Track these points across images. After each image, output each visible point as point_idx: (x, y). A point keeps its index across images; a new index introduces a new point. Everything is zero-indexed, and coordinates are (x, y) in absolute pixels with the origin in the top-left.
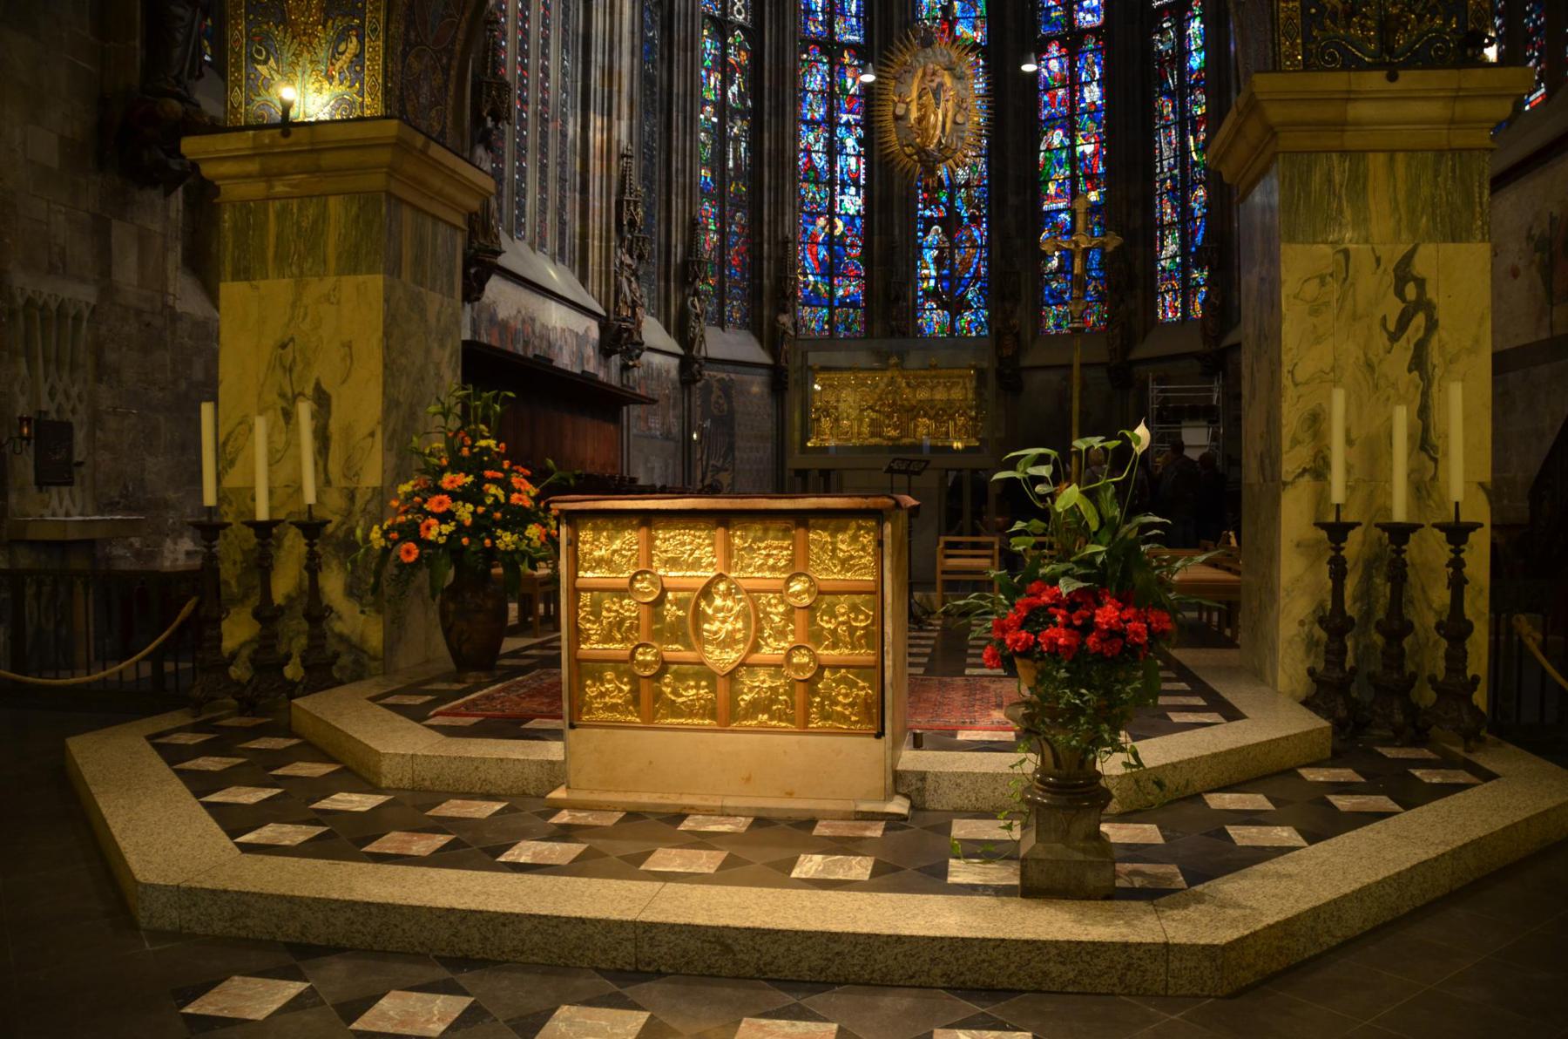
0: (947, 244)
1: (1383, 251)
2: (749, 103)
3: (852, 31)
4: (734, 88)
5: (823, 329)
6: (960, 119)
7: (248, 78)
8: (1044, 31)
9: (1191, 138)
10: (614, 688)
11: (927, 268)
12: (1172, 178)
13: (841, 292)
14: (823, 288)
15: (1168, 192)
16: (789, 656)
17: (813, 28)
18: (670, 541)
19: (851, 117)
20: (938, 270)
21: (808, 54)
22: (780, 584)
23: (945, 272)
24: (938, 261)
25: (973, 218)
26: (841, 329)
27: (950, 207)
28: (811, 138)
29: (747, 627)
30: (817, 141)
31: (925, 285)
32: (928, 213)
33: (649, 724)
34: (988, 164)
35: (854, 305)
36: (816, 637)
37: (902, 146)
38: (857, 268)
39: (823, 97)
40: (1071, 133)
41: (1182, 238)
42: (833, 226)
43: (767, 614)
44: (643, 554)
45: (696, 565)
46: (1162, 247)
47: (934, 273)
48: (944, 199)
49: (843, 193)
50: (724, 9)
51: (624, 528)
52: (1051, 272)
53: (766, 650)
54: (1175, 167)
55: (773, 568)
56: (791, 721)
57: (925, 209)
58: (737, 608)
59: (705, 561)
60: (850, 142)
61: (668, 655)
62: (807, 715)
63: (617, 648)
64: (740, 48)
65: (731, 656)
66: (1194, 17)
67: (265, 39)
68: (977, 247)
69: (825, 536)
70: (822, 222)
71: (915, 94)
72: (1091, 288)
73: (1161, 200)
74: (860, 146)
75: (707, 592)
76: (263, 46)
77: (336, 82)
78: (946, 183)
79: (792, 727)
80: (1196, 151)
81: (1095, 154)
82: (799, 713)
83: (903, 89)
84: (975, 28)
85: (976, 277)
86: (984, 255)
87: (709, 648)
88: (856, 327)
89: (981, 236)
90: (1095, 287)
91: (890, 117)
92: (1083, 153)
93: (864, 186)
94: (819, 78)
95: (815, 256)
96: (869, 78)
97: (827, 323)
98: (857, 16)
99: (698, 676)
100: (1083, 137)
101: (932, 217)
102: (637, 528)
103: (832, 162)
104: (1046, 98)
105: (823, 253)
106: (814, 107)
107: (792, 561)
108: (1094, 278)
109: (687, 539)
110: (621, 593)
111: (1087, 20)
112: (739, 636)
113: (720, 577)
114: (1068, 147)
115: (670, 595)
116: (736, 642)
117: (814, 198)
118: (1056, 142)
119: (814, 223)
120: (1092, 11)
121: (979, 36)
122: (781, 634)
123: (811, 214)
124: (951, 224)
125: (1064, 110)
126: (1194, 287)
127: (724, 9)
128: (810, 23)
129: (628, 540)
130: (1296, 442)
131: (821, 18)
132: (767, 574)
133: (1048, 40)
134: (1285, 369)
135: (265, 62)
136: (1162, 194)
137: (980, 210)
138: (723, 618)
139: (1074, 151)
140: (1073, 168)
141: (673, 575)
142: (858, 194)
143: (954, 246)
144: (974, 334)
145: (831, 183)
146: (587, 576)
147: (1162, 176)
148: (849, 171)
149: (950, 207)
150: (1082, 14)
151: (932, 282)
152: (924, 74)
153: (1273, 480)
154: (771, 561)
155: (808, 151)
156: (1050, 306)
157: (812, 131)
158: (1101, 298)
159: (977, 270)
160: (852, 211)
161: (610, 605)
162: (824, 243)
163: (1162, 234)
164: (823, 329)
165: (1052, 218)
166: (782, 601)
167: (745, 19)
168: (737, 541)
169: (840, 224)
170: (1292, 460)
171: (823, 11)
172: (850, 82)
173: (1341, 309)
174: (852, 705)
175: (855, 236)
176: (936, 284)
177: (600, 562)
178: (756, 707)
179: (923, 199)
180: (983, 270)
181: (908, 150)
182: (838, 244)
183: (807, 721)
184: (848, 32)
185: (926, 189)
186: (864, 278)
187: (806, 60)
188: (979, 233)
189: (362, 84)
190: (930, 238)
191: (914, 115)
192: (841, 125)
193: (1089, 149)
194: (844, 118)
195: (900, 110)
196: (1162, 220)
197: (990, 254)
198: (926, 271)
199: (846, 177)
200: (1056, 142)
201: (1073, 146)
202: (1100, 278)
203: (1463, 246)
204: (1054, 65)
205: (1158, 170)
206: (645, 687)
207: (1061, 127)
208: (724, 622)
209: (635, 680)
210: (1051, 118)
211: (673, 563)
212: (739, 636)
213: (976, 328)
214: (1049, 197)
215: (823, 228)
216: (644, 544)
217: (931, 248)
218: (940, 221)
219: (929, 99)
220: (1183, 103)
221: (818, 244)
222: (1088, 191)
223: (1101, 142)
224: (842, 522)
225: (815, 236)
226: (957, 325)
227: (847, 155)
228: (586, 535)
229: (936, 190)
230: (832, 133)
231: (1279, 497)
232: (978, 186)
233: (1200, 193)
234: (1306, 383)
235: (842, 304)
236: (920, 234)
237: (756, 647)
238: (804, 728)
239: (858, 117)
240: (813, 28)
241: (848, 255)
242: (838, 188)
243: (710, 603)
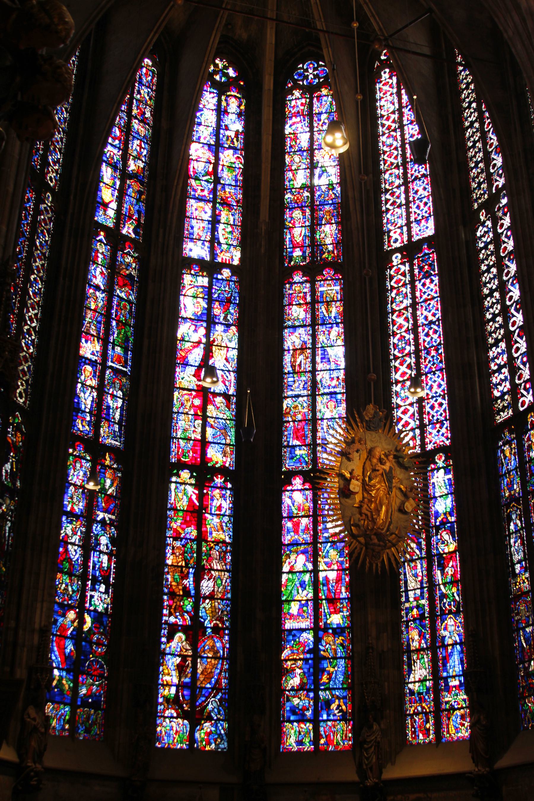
0: (190, 653)
2: (18, 484)
3: (114, 438)
4: (8, 466)
5: (63, 729)
8: (289, 465)
9: (439, 572)
11: (168, 674)
12: (418, 607)
13: (84, 691)
14: (67, 684)
15: (414, 620)
17: (80, 426)
19: (107, 516)
20: (180, 677)
21: (74, 450)
23: (187, 680)
24: (181, 668)
25: (215, 629)
26: (81, 731)
27: (195, 616)
28: (69, 532)
30: (74, 533)
31: (166, 692)
32: (172, 619)
34: (234, 580)
35: (96, 705)
38: (102, 666)
39: (83, 493)
40: (314, 557)
41: (434, 661)
42: (82, 622)
46: (410, 670)
47: (176, 681)
48: (189, 608)
49: (94, 589)
52: (292, 689)
54: (422, 596)
57: (170, 614)
60: (104, 540)
64: (17, 429)
66: (438, 469)
68: (219, 658)
70: (71, 615)
72: (334, 706)
73: (407, 627)
74: (113, 546)
78: (193, 592)
80: (445, 584)
81: (339, 580)
84: (225, 454)
85: (217, 688)
86: (226, 667)
88: (96, 729)
89: (224, 648)
90: (339, 706)
92: (326, 578)
93: (113, 585)
94: (81, 473)
95: (62, 649)
97: (68, 722)
100: (326, 563)
101: (176, 624)
103: (86, 557)
104: (289, 525)
105: (70, 647)
106: (75, 500)
108: (338, 698)
114: (311, 572)
117: (66, 589)
118: (299, 567)
119: (64, 615)
121: (229, 461)
123: (61, 605)
125: (307, 537)
126: (448, 710)
128: (79, 421)
131: (88, 419)
133: (292, 474)
136: (408, 621)
137: (223, 623)
139: (316, 577)
140: (316, 591)
142: (106, 592)
143: (196, 656)
144: (213, 746)
145: (84, 577)
147: (407, 605)
148: (101, 567)
149: (195, 616)
150: (325, 456)
151: (173, 690)
155: (65, 543)
156: (292, 722)
157: (71, 523)
158: (344, 718)
159: (218, 681)
160: (100, 609)
162: (72, 637)
163: (409, 658)
164: (63, 729)
165: (294, 636)
167: (24, 403)
169: (88, 619)
171: (90, 413)
172: (108, 482)
175: (101, 634)
176: (177, 691)
179: (170, 606)
182: (85, 639)
185: (172, 595)
186: (106, 679)
187: (72, 454)
190: (173, 644)
192: (98, 522)
193: (332, 575)
194: (101, 515)
196: (409, 645)
198: (167, 678)
199: (98, 573)
200: (299, 567)
201: (315, 571)
202: (344, 698)
205: (403, 599)
207: (304, 552)
210: (295, 544)
213: (215, 740)
214: (292, 616)
215: (73, 622)
217: (174, 655)
218: (185, 629)
220: (428, 540)
221: (67, 638)
222: (331, 613)
223: (344, 570)
225: (64, 628)
226: (197, 735)
227: (101, 552)
229: (181, 599)
230: (89, 529)
232: (222, 599)
233: (450, 622)
235: (85, 703)
236: (164, 639)
239: (113, 517)
240: (80, 426)
241: (92, 652)
242: (89, 583)
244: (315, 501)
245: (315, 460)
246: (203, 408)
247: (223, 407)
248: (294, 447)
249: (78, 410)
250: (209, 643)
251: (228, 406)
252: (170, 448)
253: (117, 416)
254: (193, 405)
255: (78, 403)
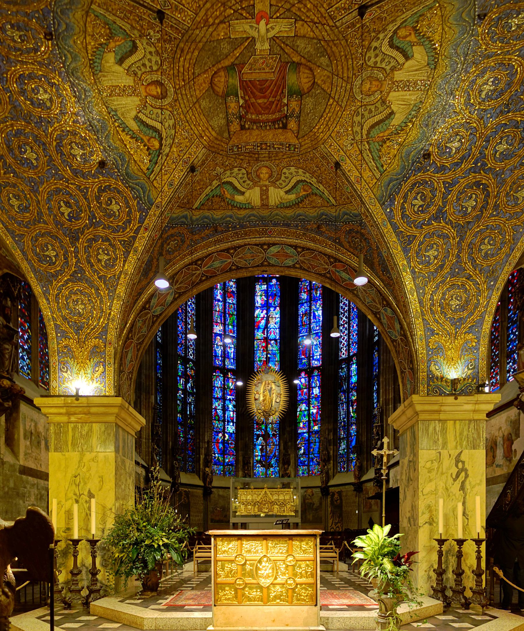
1: (452, 452)
6: (278, 401)
7: (59, 377)
10: (229, 593)
16: (287, 581)
18: (247, 544)
22: (283, 558)
24: (262, 450)
25: (273, 435)
27: (266, 430)
29: (273, 572)
33: (240, 604)
36: (295, 575)
37: (257, 410)
43: (279, 568)
44: (239, 549)
45: (257, 552)
50: (185, 354)
51: (233, 540)
53: (279, 579)
55: (282, 553)
56: (287, 602)
58: (270, 566)
59: (260, 551)
61: (247, 582)
62: (292, 599)
63: (230, 580)
65: (269, 581)
67: (65, 363)
69: (298, 543)
71: (262, 391)
75: (260, 561)
76: (64, 366)
77: (95, 382)
79: (287, 604)
82: (290, 599)
83: (258, 389)
84: (275, 365)
85: (275, 456)
87: (261, 579)
91: (253, 399)
96: (240, 384)
98: (233, 359)
99: (256, 588)
102: (238, 539)
107: (287, 551)
109: (253, 544)
110: (232, 561)
111: (315, 363)
112: (270, 575)
113: (265, 556)
115: (248, 562)
116: (269, 577)
120: (318, 360)
122: (284, 574)
124: (266, 436)
127: (185, 354)
129: (234, 544)
130: (423, 513)
132: (280, 555)
133: (301, 371)
134: (420, 490)
135: (66, 372)
138: (266, 569)
141: (249, 556)
143: (266, 446)
146: (220, 556)
149: (266, 430)
152: (265, 384)
153: (415, 525)
154: (281, 551)
159: (275, 453)
161: (228, 566)
166: (284, 563)
168: (270, 545)
170: (422, 519)
173: (438, 471)
174: (307, 596)
177: (224, 552)
178: (276, 597)
180: (277, 454)
181: (259, 411)
183: (292, 602)
184: (230, 365)
188: (276, 440)
189: (105, 383)
191: (262, 398)
195: (257, 397)
197: (279, 447)
203: (477, 451)
204: (303, 380)
206: (240, 593)
208: (266, 570)
209: (236, 590)
211: (249, 551)
212: (270, 575)
216: (239, 546)
219: (267, 393)
224: (303, 539)
228: (219, 543)
231: (418, 530)
234: (427, 495)
237: (276, 578)
238: (291, 604)
243: (261, 564)
244: (309, 381)
245: (310, 364)
246: (266, 347)
247: (274, 345)
248: (302, 359)
249: (216, 356)
250: (271, 440)
251: (276, 344)
252: (254, 365)
253: (232, 356)
254: (262, 346)
255: (216, 353)
